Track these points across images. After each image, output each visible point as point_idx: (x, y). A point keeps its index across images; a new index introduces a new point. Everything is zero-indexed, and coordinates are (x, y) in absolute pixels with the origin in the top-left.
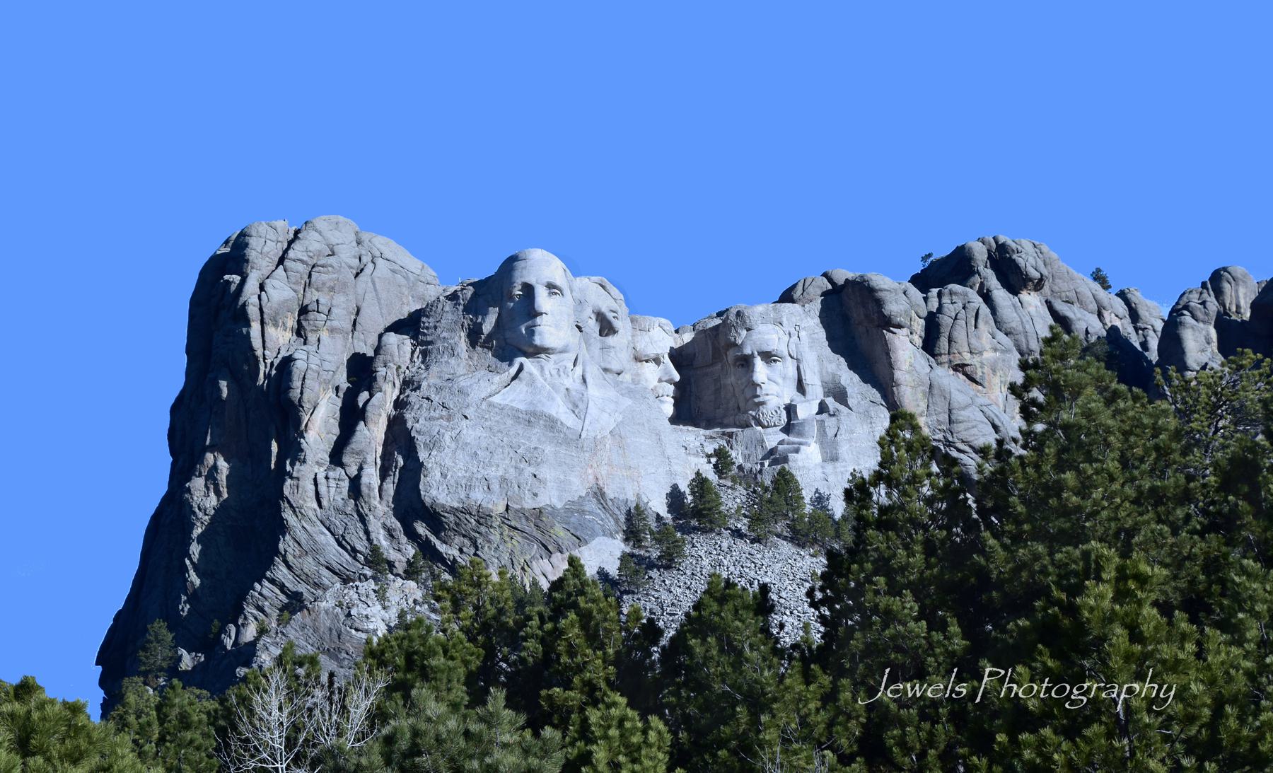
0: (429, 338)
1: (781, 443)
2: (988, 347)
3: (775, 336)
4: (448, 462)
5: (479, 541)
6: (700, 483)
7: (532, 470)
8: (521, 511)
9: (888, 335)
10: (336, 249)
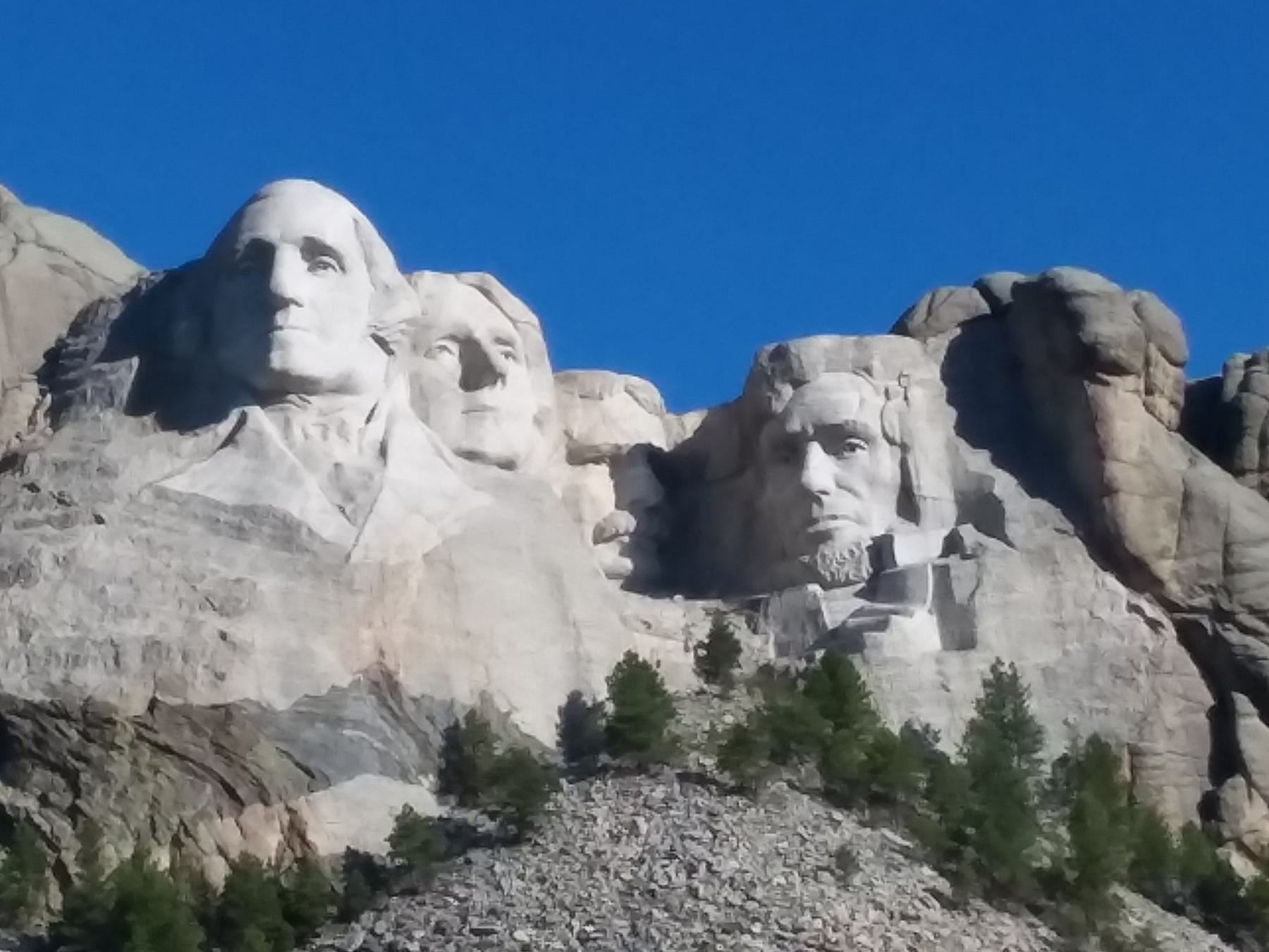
1: (858, 613)
4: (37, 609)
5: (85, 777)
6: (634, 678)
7: (222, 624)
8: (185, 713)
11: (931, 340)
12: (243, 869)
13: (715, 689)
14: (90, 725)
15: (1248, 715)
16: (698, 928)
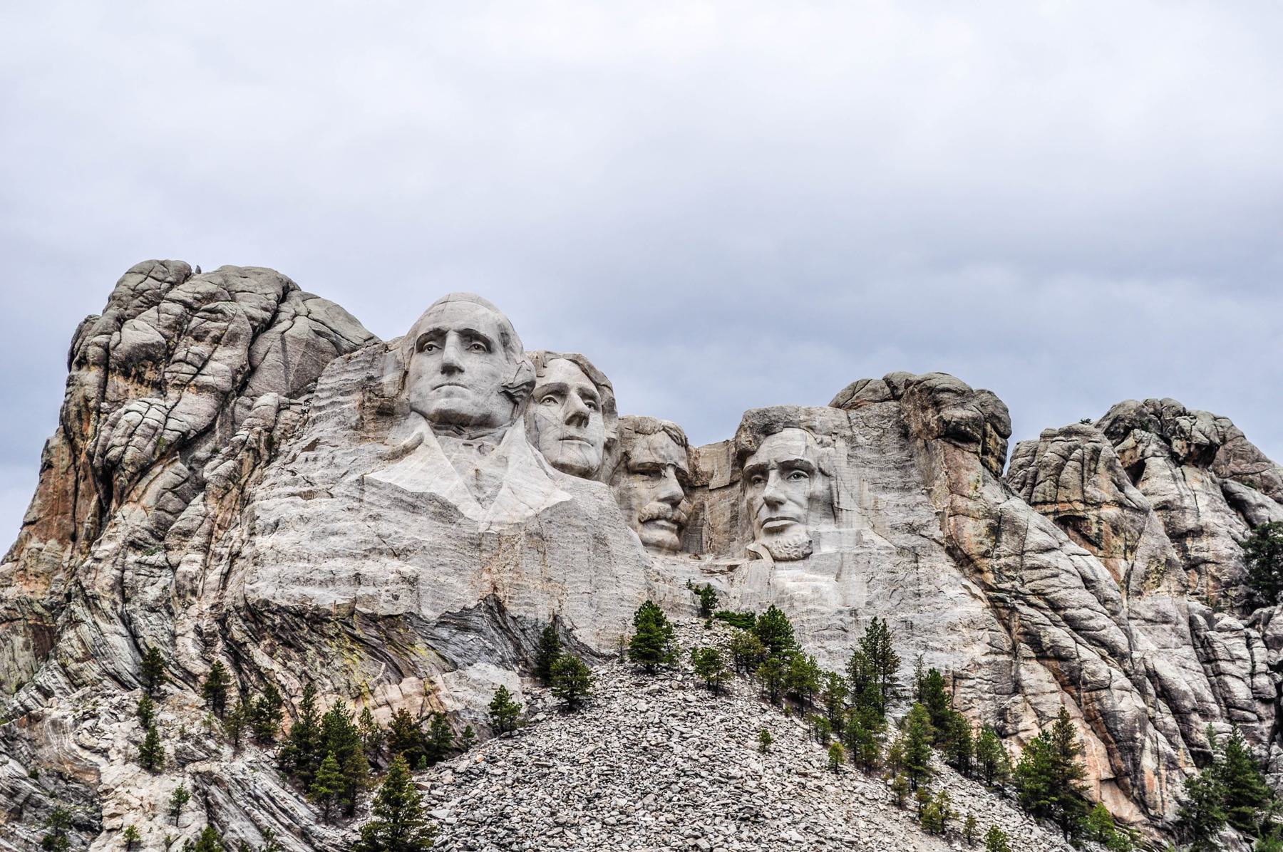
0: (323, 403)
2: (1109, 498)
3: (802, 444)
8: (372, 619)
9: (950, 448)
10: (239, 296)
11: (853, 413)
12: (402, 719)
13: (703, 621)
14: (316, 623)
15: (1030, 658)
16: (671, 771)
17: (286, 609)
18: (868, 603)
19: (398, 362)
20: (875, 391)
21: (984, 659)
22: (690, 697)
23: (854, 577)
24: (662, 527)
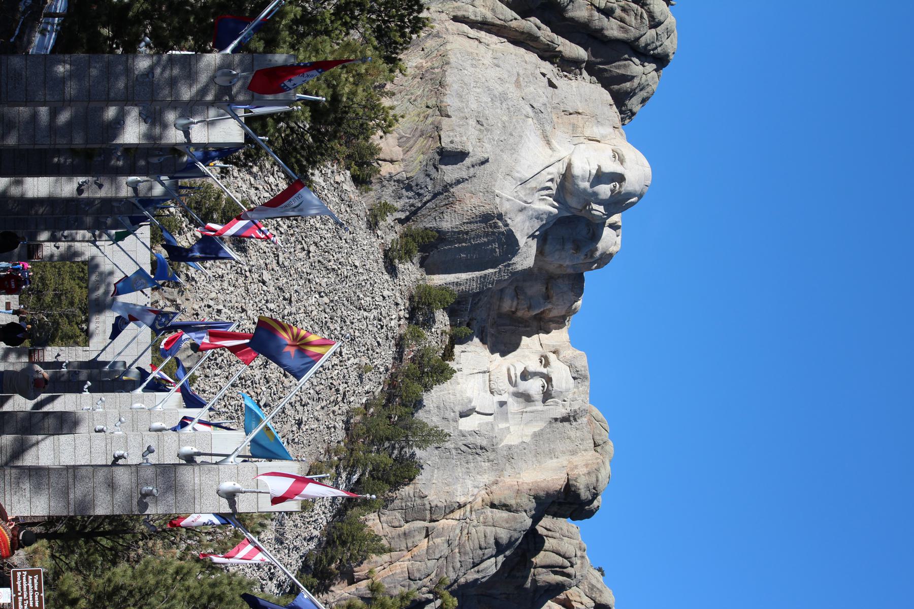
8: (438, 128)
17: (444, 75)
18: (461, 431)
19: (606, 136)
20: (600, 435)
21: (427, 503)
22: (393, 323)
23: (477, 422)
24: (513, 301)
